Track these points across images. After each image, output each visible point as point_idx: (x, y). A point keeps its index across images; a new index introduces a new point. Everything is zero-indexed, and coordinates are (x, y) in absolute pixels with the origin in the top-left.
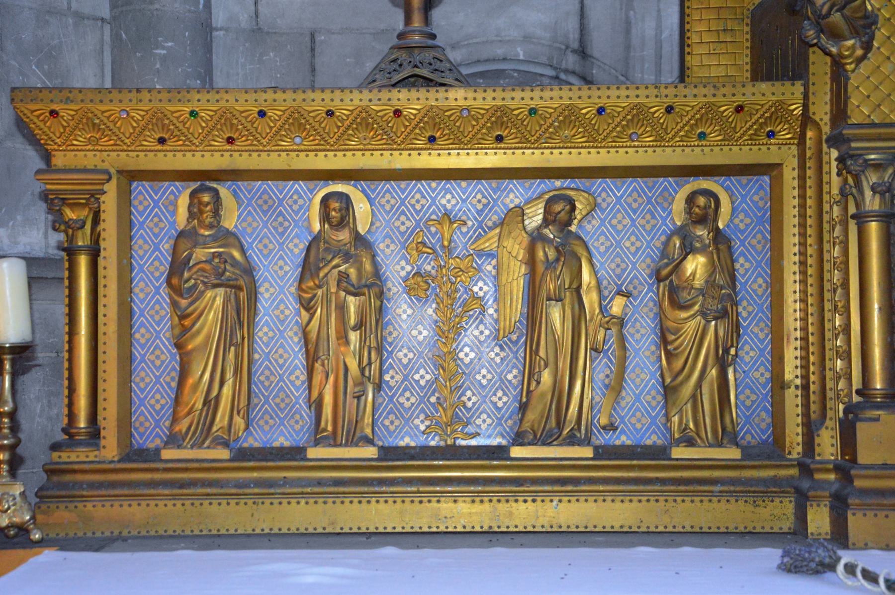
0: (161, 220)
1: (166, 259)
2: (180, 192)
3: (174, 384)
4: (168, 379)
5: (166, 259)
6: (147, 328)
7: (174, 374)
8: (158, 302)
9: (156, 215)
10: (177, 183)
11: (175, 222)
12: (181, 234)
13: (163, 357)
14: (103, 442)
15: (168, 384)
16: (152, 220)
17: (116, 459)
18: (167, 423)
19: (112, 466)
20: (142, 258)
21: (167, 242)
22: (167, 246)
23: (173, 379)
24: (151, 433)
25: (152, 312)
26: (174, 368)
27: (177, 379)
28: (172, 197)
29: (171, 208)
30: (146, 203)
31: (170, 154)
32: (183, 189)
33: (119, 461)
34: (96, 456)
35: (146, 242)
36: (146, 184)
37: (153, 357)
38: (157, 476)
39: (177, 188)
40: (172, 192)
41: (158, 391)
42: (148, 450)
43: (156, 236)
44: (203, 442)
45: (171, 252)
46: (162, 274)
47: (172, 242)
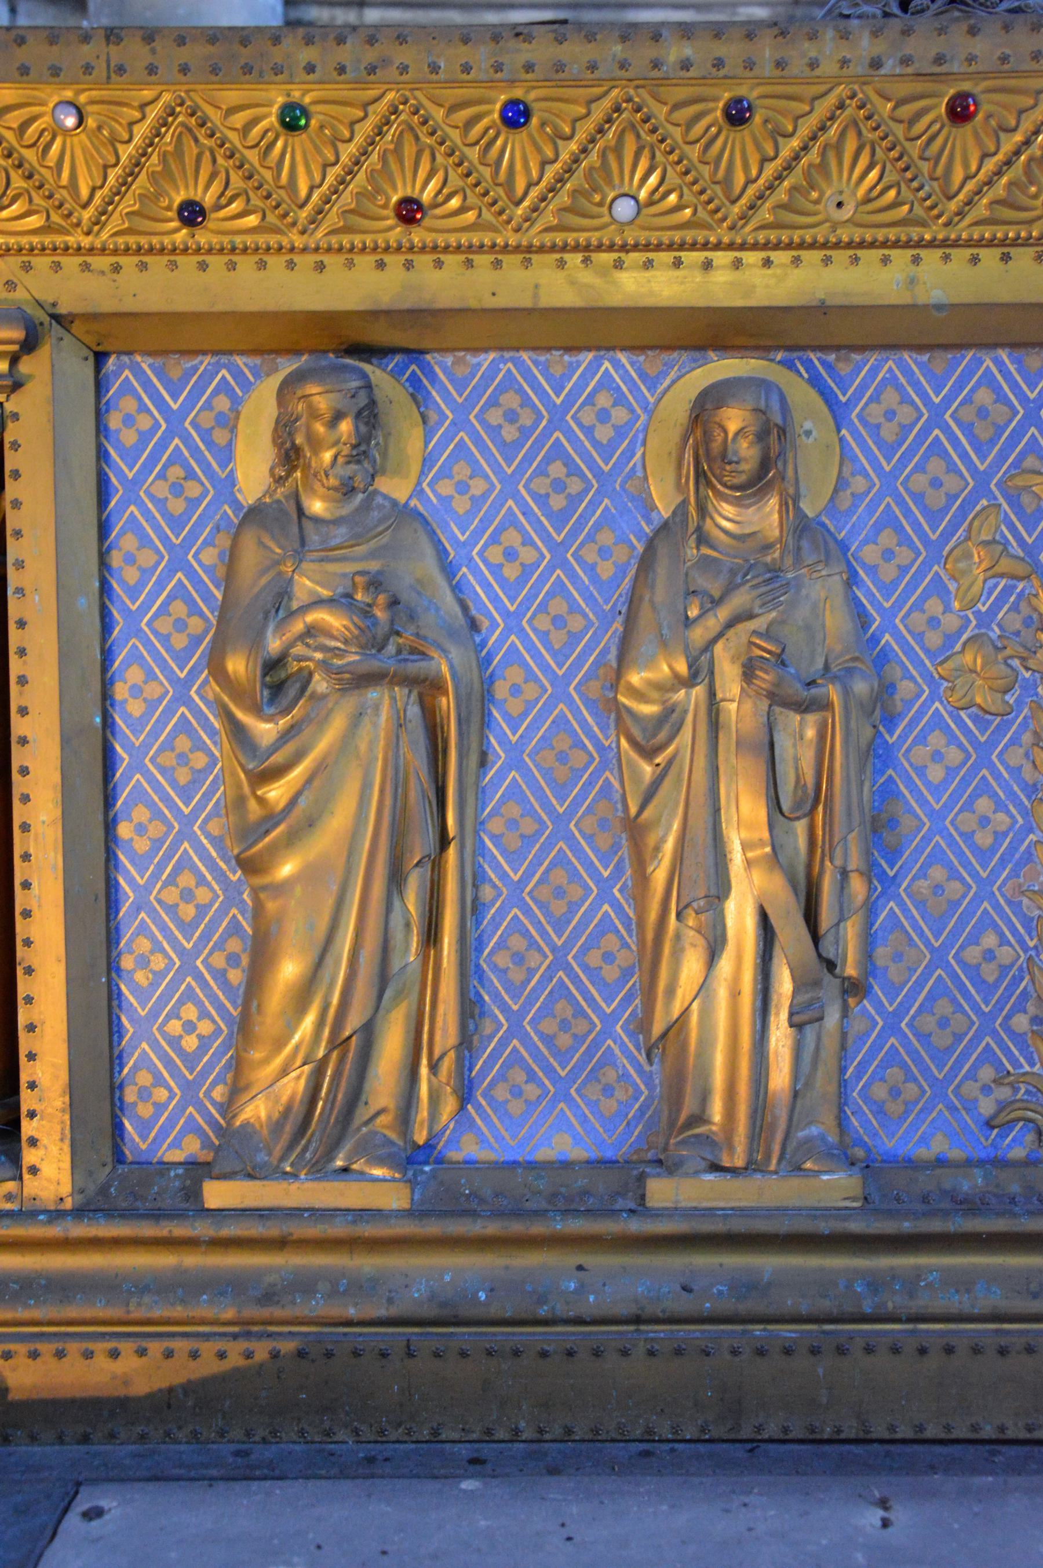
0: (190, 475)
1: (207, 597)
2: (247, 386)
3: (236, 976)
4: (219, 960)
5: (207, 597)
6: (151, 805)
7: (234, 945)
8: (184, 726)
9: (176, 458)
10: (239, 360)
11: (231, 479)
12: (255, 515)
13: (202, 895)
14: (29, 1156)
15: (220, 976)
16: (162, 476)
17: (68, 1204)
18: (219, 1093)
19: (55, 1231)
20: (133, 593)
21: (208, 543)
22: (209, 556)
23: (233, 960)
24: (172, 1121)
25: (168, 759)
26: (235, 928)
27: (245, 961)
28: (223, 403)
29: (220, 437)
30: (144, 423)
31: (216, 262)
32: (257, 375)
33: (79, 1213)
34: (9, 1197)
35: (145, 541)
36: (145, 364)
37: (171, 895)
38: (192, 1260)
39: (238, 374)
40: (224, 387)
41: (189, 992)
42: (166, 1166)
43: (177, 523)
44: (330, 1154)
45: (221, 572)
46: (197, 641)
47: (224, 541)
